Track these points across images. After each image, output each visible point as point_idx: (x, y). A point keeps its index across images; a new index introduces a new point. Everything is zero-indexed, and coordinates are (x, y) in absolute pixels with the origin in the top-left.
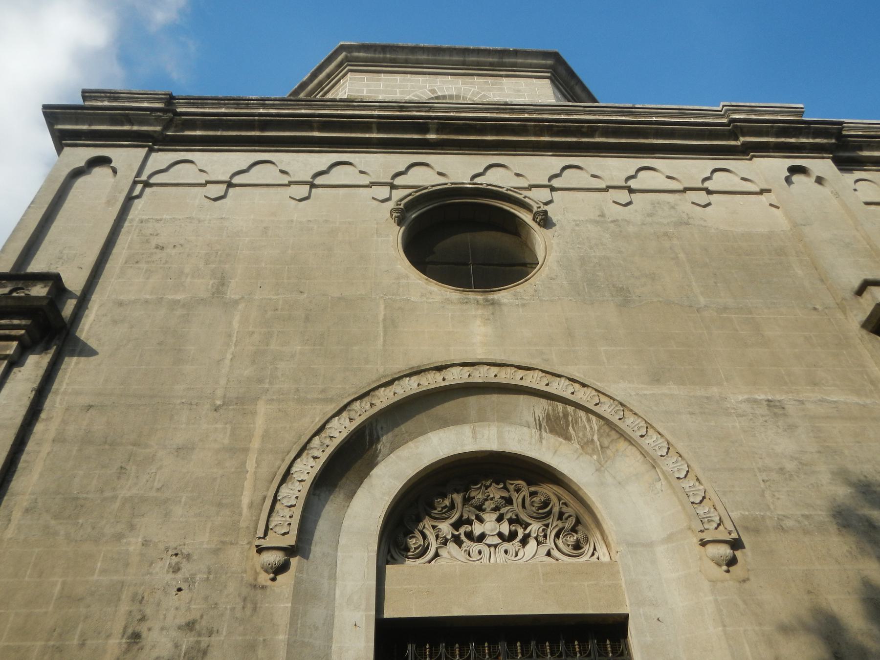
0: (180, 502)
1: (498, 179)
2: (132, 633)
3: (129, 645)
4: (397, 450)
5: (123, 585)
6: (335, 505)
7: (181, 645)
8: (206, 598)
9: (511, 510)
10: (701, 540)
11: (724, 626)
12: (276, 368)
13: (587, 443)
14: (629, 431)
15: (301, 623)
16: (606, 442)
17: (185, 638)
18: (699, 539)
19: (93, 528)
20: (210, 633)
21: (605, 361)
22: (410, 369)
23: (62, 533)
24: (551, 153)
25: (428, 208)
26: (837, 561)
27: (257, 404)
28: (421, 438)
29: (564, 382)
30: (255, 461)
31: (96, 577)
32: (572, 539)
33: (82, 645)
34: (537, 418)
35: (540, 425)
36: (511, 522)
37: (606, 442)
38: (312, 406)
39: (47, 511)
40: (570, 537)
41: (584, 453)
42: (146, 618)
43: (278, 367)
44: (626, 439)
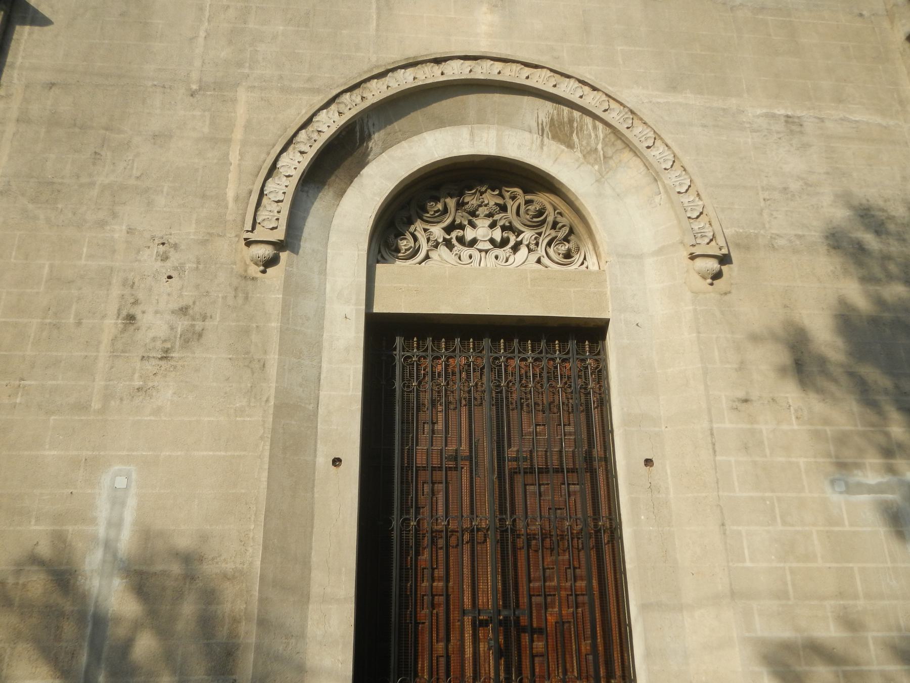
0: (162, 192)
2: (127, 315)
3: (125, 324)
5: (112, 270)
6: (324, 203)
7: (176, 328)
8: (197, 286)
9: (505, 217)
10: (691, 254)
11: (699, 333)
12: (256, 50)
13: (589, 153)
14: (635, 141)
15: (292, 313)
16: (610, 152)
17: (180, 321)
19: (74, 214)
20: (204, 318)
21: (621, 62)
23: (42, 217)
27: (237, 91)
28: (415, 138)
29: (573, 84)
30: (238, 153)
31: (83, 262)
33: (79, 324)
34: (540, 122)
36: (504, 228)
37: (610, 152)
38: (297, 96)
39: (23, 195)
40: (561, 246)
42: (139, 302)
43: (258, 49)
44: (631, 150)
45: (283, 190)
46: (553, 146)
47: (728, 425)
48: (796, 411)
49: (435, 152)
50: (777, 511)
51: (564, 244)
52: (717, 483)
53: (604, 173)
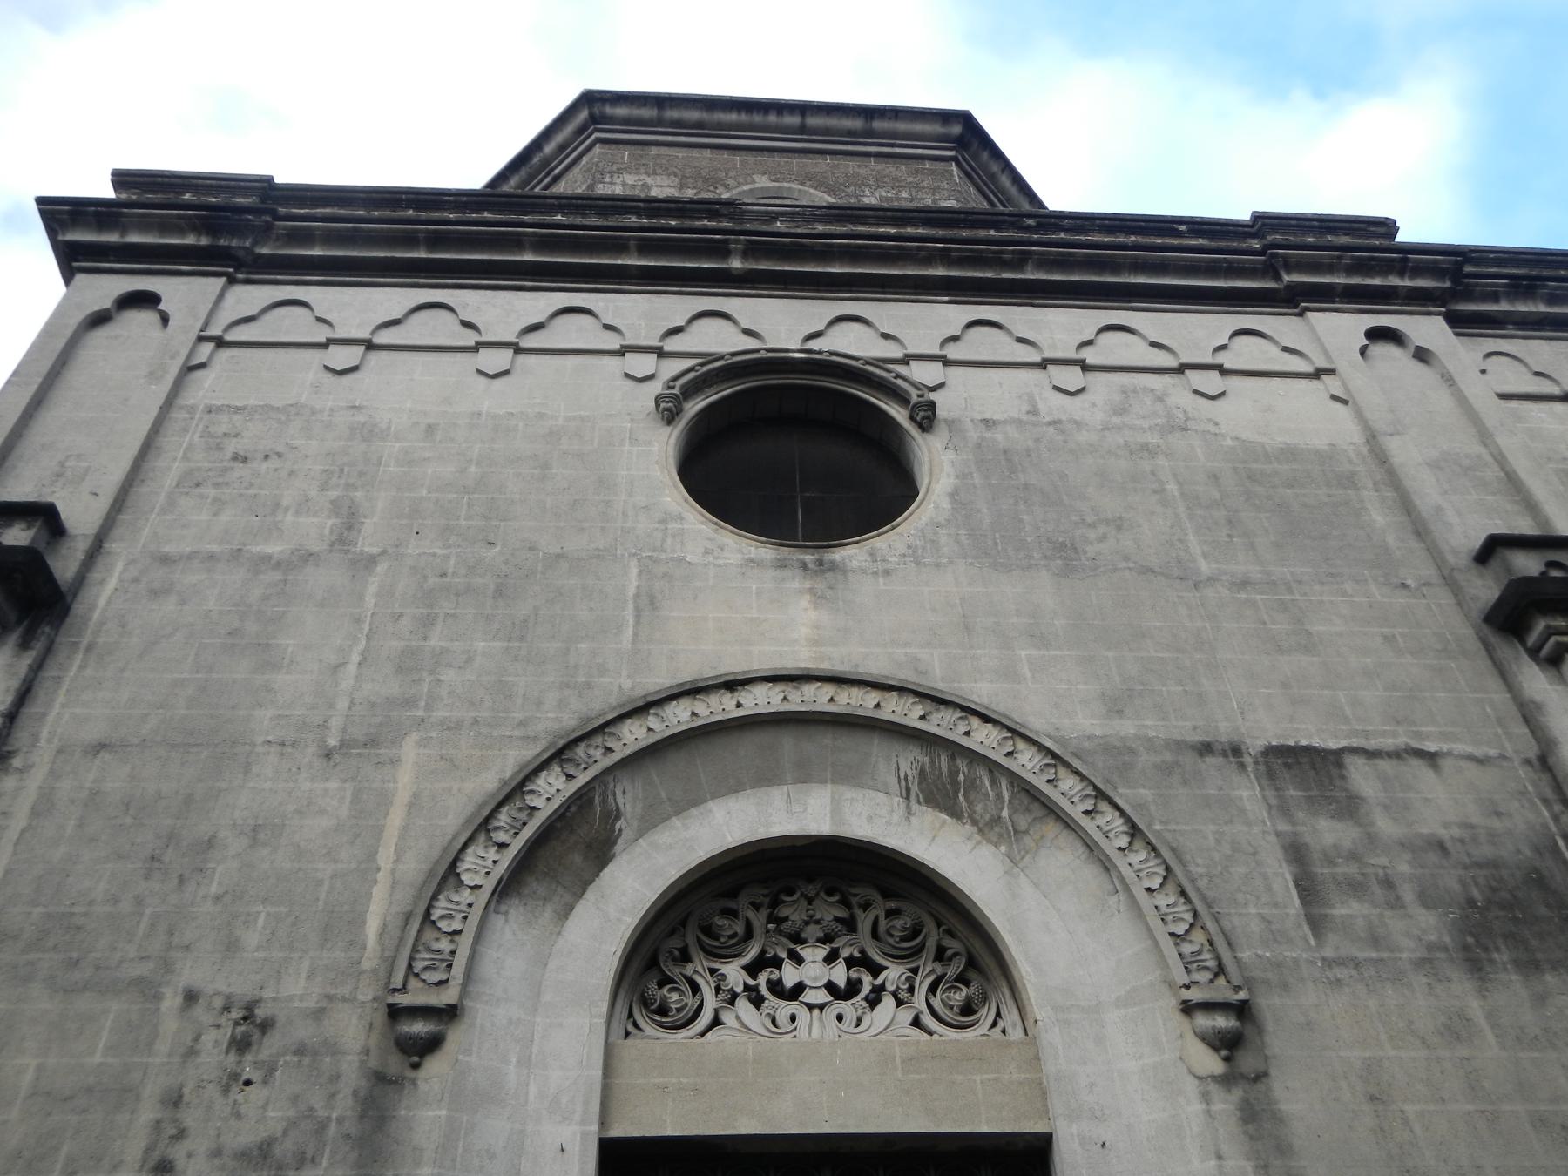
1: (852, 343)
4: (650, 832)
5: (145, 1074)
6: (534, 932)
8: (295, 1099)
9: (851, 942)
10: (1184, 1002)
11: (1220, 1157)
12: (439, 680)
14: (1064, 803)
15: (463, 1146)
18: (1180, 1001)
21: (1028, 675)
22: (677, 685)
24: (946, 298)
25: (725, 393)
26: (1424, 1043)
27: (401, 746)
28: (694, 811)
29: (950, 715)
30: (392, 850)
32: (957, 996)
34: (902, 776)
35: (908, 790)
36: (851, 963)
37: (1023, 822)
38: (500, 750)
40: (955, 993)
43: (442, 678)
44: (1058, 818)
45: (464, 912)
46: (928, 817)
49: (727, 834)
51: (959, 988)
53: (1018, 858)
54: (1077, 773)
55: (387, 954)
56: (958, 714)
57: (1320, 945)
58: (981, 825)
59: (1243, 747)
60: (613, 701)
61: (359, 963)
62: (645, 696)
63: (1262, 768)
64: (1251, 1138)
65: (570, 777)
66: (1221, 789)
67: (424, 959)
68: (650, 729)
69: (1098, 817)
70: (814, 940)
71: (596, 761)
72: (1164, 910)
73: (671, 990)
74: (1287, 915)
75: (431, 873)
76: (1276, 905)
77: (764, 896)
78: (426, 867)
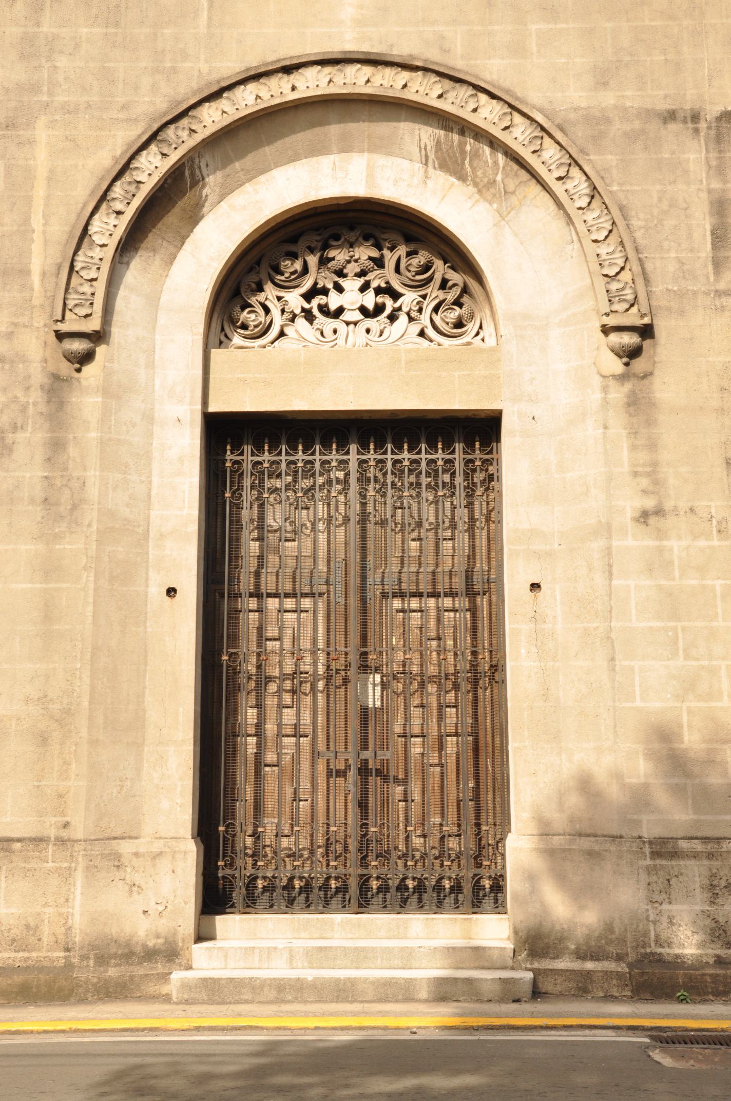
6: (149, 275)
10: (603, 326)
11: (606, 428)
12: (55, 67)
16: (511, 187)
27: (35, 128)
28: (262, 178)
29: (464, 92)
30: (41, 215)
32: (452, 315)
34: (423, 147)
35: (427, 157)
37: (511, 185)
38: (110, 131)
41: (482, 200)
43: (58, 64)
44: (538, 181)
46: (441, 179)
47: (630, 542)
48: (719, 523)
50: (681, 644)
52: (610, 612)
53: (505, 213)
54: (558, 143)
55: (49, 294)
56: (471, 91)
57: (716, 281)
58: (480, 187)
59: (702, 114)
60: (195, 85)
61: (31, 300)
62: (218, 82)
63: (713, 132)
64: (630, 415)
65: (164, 155)
66: (673, 153)
67: (74, 299)
68: (224, 112)
69: (569, 181)
70: (353, 275)
71: (183, 142)
72: (604, 257)
73: (249, 312)
74: (699, 258)
75: (71, 234)
76: (692, 251)
77: (317, 241)
78: (67, 228)
